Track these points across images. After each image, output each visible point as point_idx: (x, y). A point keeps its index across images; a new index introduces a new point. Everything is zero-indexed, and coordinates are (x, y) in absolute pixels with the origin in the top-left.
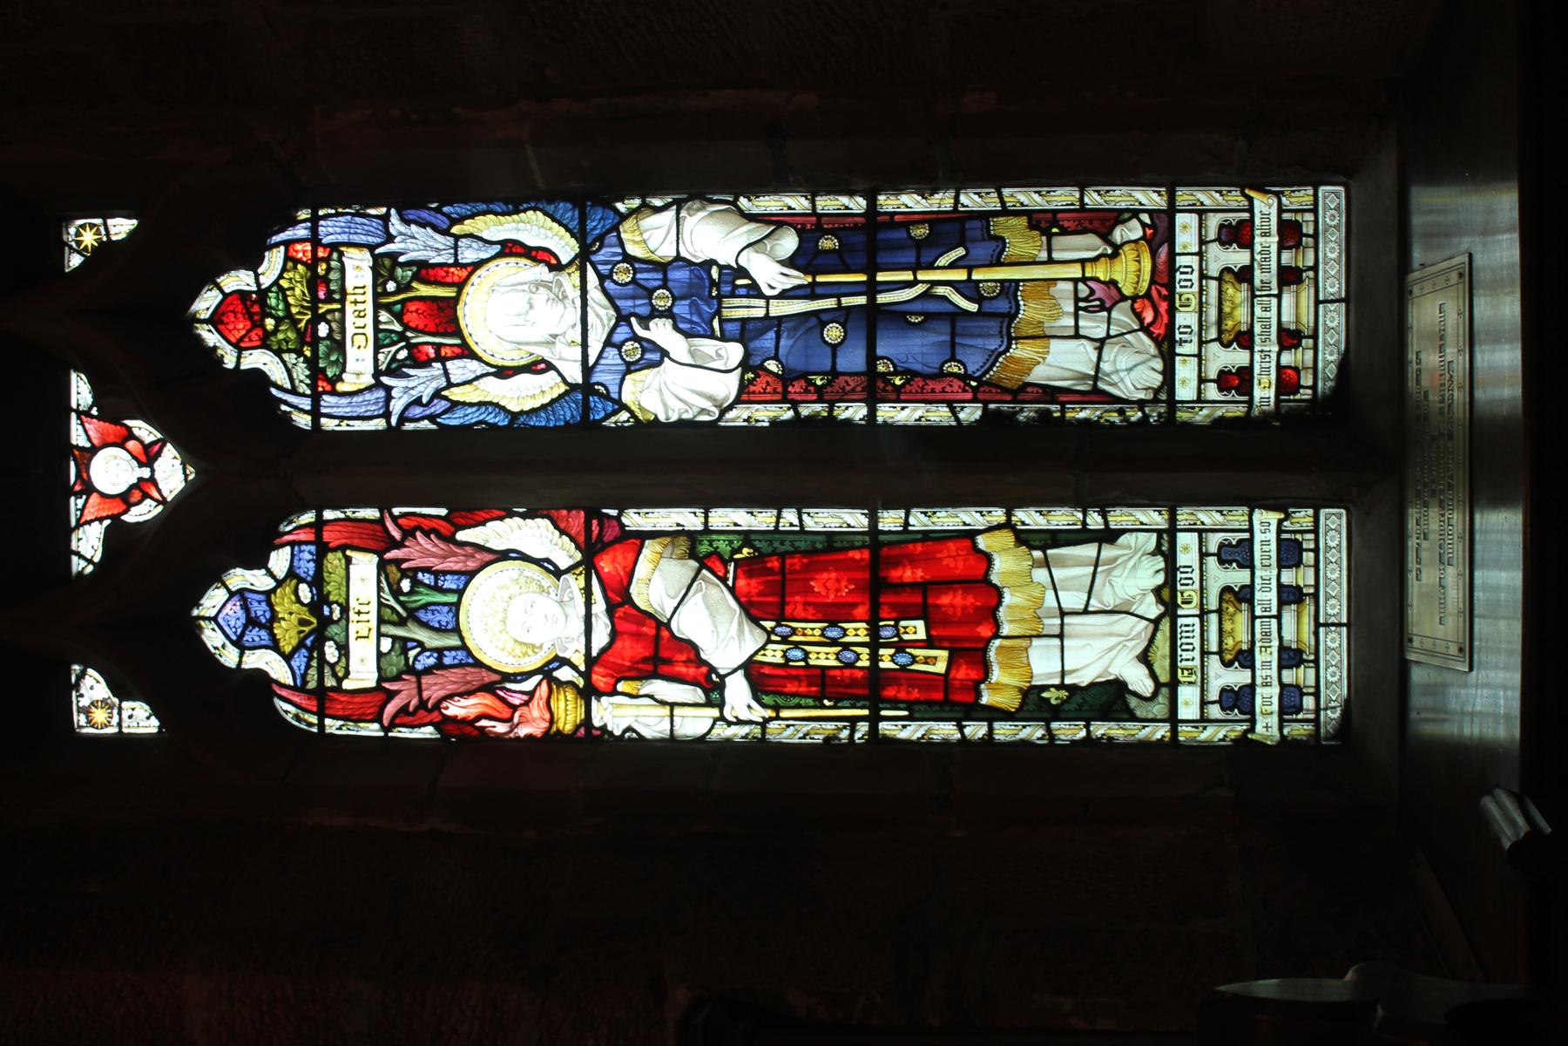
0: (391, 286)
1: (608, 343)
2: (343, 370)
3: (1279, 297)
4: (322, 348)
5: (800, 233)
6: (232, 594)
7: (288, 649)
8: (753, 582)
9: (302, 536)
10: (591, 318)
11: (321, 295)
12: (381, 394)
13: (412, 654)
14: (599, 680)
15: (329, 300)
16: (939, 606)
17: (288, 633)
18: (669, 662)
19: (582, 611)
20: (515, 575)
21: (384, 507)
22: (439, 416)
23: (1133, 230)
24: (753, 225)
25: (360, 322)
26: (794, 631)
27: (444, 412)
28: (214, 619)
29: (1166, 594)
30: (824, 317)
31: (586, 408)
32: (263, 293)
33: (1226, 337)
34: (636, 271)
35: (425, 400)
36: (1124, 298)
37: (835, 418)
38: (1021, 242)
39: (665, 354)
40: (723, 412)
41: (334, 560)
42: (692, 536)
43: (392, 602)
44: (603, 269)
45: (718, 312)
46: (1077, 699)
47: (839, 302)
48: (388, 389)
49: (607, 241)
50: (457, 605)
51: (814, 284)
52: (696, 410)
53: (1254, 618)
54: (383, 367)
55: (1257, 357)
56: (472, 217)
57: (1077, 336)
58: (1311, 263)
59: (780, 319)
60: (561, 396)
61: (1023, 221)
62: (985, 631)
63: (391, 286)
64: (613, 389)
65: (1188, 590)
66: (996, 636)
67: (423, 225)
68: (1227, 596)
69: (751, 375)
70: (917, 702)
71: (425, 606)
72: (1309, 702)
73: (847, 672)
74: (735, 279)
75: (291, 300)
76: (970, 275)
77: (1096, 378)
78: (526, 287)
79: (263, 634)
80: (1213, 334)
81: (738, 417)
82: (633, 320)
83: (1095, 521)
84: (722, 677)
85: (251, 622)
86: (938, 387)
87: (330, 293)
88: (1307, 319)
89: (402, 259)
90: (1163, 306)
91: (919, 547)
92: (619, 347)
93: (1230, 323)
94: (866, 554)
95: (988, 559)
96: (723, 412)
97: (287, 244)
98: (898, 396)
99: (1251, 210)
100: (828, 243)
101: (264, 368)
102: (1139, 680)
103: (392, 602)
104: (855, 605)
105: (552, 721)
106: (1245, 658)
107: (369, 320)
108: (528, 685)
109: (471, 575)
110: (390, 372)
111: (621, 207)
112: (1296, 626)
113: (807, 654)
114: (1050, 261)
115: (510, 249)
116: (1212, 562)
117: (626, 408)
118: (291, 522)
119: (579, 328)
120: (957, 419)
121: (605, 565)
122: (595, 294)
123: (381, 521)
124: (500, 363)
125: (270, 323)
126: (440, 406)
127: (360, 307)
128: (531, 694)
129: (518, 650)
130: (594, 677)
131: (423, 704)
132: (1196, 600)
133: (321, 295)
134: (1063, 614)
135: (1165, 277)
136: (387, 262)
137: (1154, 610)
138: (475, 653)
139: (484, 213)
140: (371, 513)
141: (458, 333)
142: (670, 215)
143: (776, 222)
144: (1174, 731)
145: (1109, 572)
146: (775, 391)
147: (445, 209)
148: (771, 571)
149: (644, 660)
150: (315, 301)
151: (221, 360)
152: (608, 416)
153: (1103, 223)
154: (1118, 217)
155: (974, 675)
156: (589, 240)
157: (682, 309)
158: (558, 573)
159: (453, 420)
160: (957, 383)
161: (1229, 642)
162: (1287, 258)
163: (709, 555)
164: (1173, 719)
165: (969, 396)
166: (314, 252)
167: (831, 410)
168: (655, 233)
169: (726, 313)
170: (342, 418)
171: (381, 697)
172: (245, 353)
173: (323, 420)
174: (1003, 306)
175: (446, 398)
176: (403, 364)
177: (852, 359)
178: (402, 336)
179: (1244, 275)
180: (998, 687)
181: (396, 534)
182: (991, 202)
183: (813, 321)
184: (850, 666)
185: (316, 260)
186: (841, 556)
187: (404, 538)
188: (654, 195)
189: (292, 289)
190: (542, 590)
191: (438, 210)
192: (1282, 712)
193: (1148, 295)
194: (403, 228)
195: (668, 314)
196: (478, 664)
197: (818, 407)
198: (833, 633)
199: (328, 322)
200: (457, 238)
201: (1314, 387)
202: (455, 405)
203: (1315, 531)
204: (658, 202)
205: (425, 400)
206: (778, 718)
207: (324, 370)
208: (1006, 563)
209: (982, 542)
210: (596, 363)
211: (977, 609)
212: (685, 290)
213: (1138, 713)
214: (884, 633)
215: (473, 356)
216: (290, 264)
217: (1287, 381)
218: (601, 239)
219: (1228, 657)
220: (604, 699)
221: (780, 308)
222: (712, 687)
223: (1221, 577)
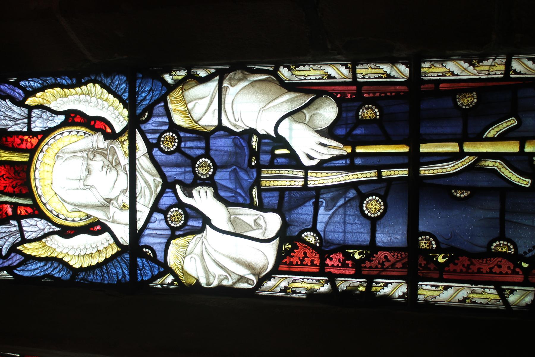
1: (155, 208)
5: (339, 103)
10: (140, 184)
24: (292, 95)
27: (19, 265)
30: (364, 189)
34: (180, 140)
37: (374, 294)
39: (206, 221)
40: (261, 281)
45: (257, 182)
47: (379, 174)
49: (155, 111)
51: (353, 155)
52: (235, 278)
56: (42, 89)
59: (319, 190)
60: (113, 257)
64: (160, 256)
69: (288, 246)
74: (270, 150)
76: (522, 147)
78: (85, 154)
81: (276, 285)
82: (178, 187)
86: (485, 269)
92: (165, 213)
96: (261, 281)
98: (440, 275)
100: (368, 113)
111: (168, 78)
115: (74, 119)
117: (169, 270)
120: (506, 302)
122: (143, 162)
124: (64, 223)
126: (17, 259)
139: (52, 86)
141: (29, 194)
142: (213, 85)
143: (316, 91)
146: (313, 264)
147: (22, 83)
152: (155, 278)
156: (138, 111)
157: (222, 177)
165: (519, 278)
167: (369, 287)
168: (198, 104)
169: (265, 183)
175: (20, 252)
177: (392, 235)
183: (352, 194)
188: (199, 67)
191: (16, 84)
195: (210, 182)
197: (355, 282)
200: (30, 108)
202: (29, 259)
204: (202, 73)
210: (145, 227)
212: (226, 158)
215: (42, 216)
218: (150, 109)
221: (318, 179)
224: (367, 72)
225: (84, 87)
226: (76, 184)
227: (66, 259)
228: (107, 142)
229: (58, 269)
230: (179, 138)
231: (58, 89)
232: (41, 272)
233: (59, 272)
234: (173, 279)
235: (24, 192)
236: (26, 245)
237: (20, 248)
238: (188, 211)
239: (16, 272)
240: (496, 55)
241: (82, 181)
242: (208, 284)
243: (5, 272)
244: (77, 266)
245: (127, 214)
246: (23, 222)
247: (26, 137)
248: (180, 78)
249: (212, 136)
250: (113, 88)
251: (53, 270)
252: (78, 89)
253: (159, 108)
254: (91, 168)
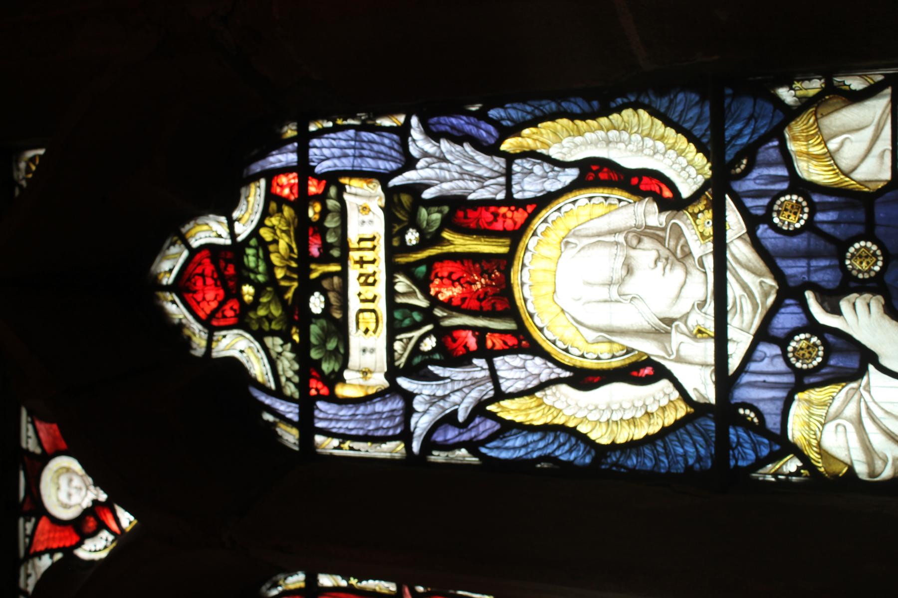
0: (412, 237)
1: (763, 335)
2: (345, 366)
4: (314, 329)
10: (733, 290)
11: (315, 251)
12: (397, 404)
15: (325, 259)
22: (484, 443)
25: (368, 292)
31: (723, 446)
32: (237, 248)
34: (814, 208)
35: (461, 417)
39: (868, 357)
44: (756, 205)
48: (408, 397)
49: (761, 156)
54: (401, 362)
60: (679, 424)
63: (412, 237)
64: (773, 423)
67: (458, 138)
75: (274, 259)
78: (620, 238)
82: (809, 296)
87: (326, 247)
89: (427, 194)
92: (783, 342)
97: (271, 175)
101: (242, 358)
107: (380, 289)
111: (786, 95)
115: (596, 174)
118: (275, 585)
119: (710, 308)
122: (739, 250)
125: (248, 291)
126: (486, 427)
127: (368, 269)
133: (315, 251)
136: (405, 199)
139: (553, 117)
141: (512, 311)
150: (305, 260)
151: (187, 343)
152: (761, 462)
156: (730, 155)
159: (511, 449)
166: (303, 186)
170: (344, 437)
172: (218, 335)
173: (319, 439)
175: (493, 416)
176: (429, 358)
178: (428, 316)
185: (302, 202)
188: (850, 71)
189: (275, 242)
191: (482, 115)
199: (324, 292)
200: (510, 158)
202: (508, 427)
204: (856, 84)
205: (461, 417)
207: (318, 363)
215: (536, 350)
216: (273, 206)
218: (751, 152)
225: (615, 117)
226: (604, 293)
227: (582, 429)
228: (664, 217)
229: (567, 447)
230: (811, 205)
231: (565, 121)
232: (533, 451)
233: (570, 451)
234: (800, 464)
235: (499, 307)
236: (505, 403)
237: (491, 408)
238: (831, 339)
239: (483, 450)
241: (614, 289)
242: (872, 474)
243: (463, 452)
244: (605, 441)
245: (710, 345)
246: (498, 361)
247: (503, 210)
248: (811, 93)
249: (880, 200)
250: (675, 117)
251: (558, 447)
252: (603, 121)
253: (771, 150)
254: (633, 263)
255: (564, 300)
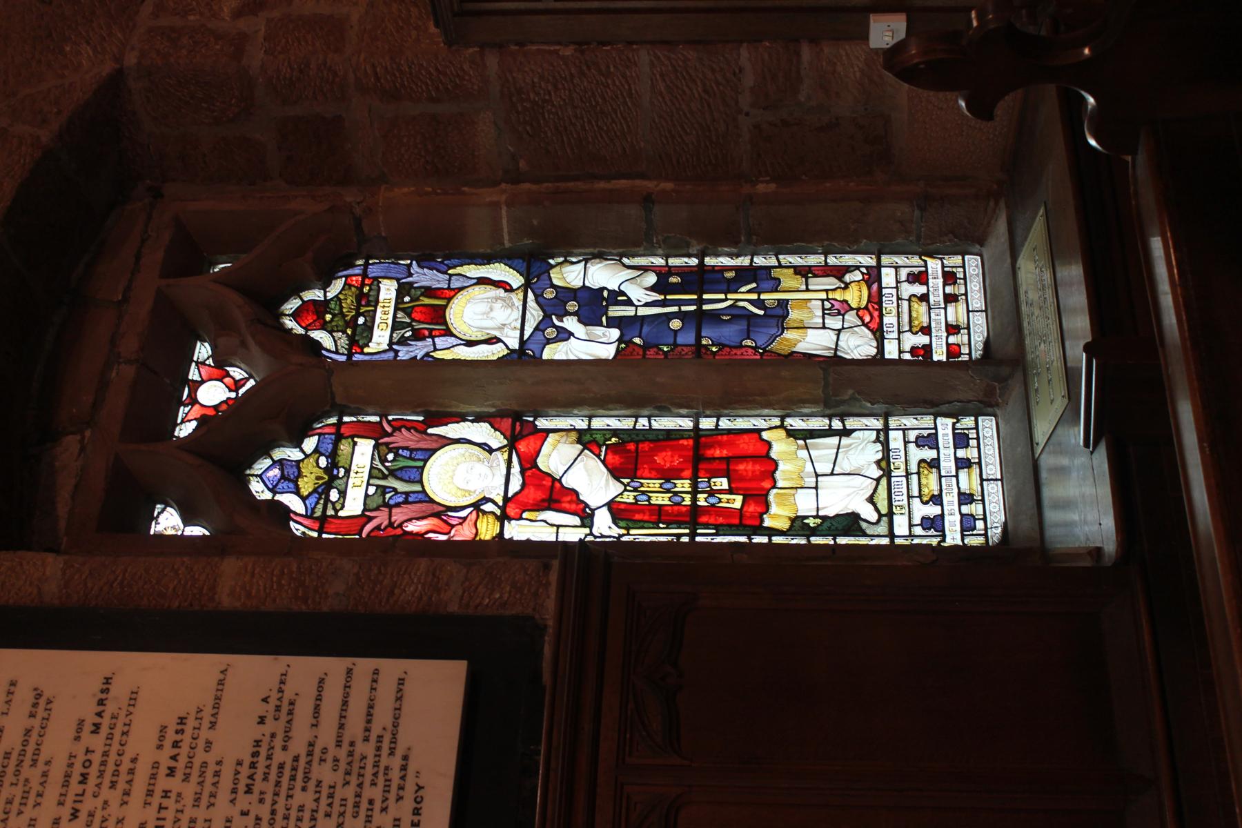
1: (537, 329)
3: (945, 309)
4: (359, 330)
6: (274, 462)
7: (306, 493)
8: (617, 458)
9: (327, 430)
10: (528, 315)
13: (388, 496)
14: (511, 511)
15: (368, 305)
16: (736, 471)
17: (306, 485)
18: (559, 502)
19: (504, 472)
20: (463, 451)
21: (383, 416)
23: (857, 276)
26: (642, 485)
28: (260, 476)
29: (883, 464)
32: (327, 301)
33: (914, 330)
36: (852, 309)
38: (789, 280)
39: (572, 334)
41: (344, 447)
42: (580, 432)
43: (380, 467)
44: (538, 292)
45: (606, 314)
46: (827, 524)
50: (423, 468)
53: (941, 477)
55: (934, 339)
56: (462, 265)
57: (824, 327)
58: (963, 291)
59: (644, 317)
61: (792, 271)
62: (766, 485)
63: (407, 299)
65: (898, 462)
66: (774, 487)
68: (923, 465)
70: (721, 525)
71: (401, 469)
72: (980, 524)
73: (676, 508)
74: (617, 297)
77: (836, 350)
79: (291, 485)
80: (907, 328)
83: (837, 425)
84: (593, 510)
85: (283, 477)
88: (963, 320)
90: (876, 314)
91: (725, 438)
93: (916, 323)
94: (691, 442)
95: (769, 445)
99: (926, 266)
102: (868, 513)
103: (380, 467)
104: (682, 470)
105: (476, 534)
106: (937, 499)
108: (463, 514)
109: (434, 451)
110: (399, 343)
111: (551, 261)
112: (968, 481)
113: (650, 498)
114: (807, 290)
115: (482, 281)
116: (912, 446)
121: (522, 447)
123: (380, 423)
128: (465, 519)
129: (459, 493)
130: (508, 510)
131: (391, 524)
132: (903, 467)
134: (817, 476)
135: (876, 300)
137: (877, 473)
138: (432, 496)
140: (375, 419)
141: (445, 323)
143: (645, 269)
144: (892, 541)
145: (846, 452)
148: (629, 451)
149: (543, 500)
153: (839, 272)
154: (848, 269)
155: (759, 510)
158: (491, 451)
160: (750, 351)
161: (925, 491)
162: (949, 290)
163: (590, 442)
164: (891, 535)
166: (363, 281)
168: (570, 275)
171: (363, 520)
174: (780, 312)
176: (408, 338)
179: (924, 298)
180: (775, 517)
181: (389, 429)
182: (773, 261)
184: (679, 504)
186: (675, 443)
187: (394, 431)
190: (479, 460)
192: (962, 531)
193: (866, 308)
194: (419, 270)
196: (432, 501)
198: (668, 486)
200: (451, 275)
201: (970, 354)
203: (977, 428)
204: (574, 260)
206: (628, 534)
208: (780, 447)
209: (765, 435)
211: (762, 472)
213: (868, 532)
214: (700, 485)
215: (452, 335)
217: (953, 351)
219: (925, 499)
220: (513, 522)
221: (643, 312)
222: (586, 516)
223: (916, 454)
224: (673, 261)
240: (746, 255)
246: (436, 340)
255: (465, 319)
